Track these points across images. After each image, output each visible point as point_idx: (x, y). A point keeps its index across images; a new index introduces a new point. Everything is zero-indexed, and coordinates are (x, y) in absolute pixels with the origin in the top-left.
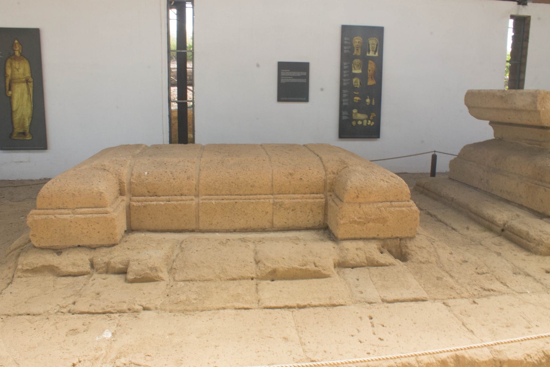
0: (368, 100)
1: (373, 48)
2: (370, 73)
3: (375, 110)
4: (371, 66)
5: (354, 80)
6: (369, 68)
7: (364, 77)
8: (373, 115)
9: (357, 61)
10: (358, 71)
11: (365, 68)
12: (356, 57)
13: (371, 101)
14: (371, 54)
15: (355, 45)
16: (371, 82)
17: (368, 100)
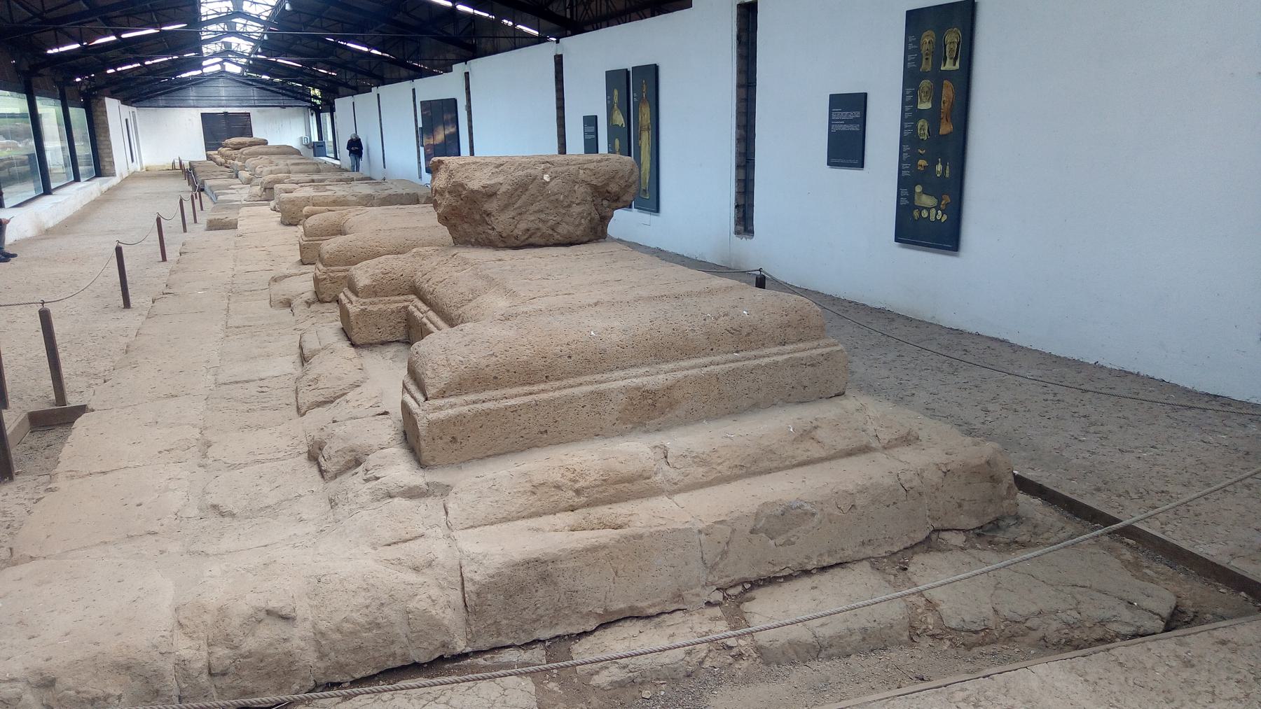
0: (939, 168)
1: (951, 50)
2: (945, 107)
3: (952, 190)
4: (948, 92)
5: (920, 123)
6: (944, 98)
7: (934, 117)
8: (946, 199)
9: (925, 84)
10: (925, 105)
11: (937, 100)
12: (925, 75)
13: (944, 169)
14: (948, 66)
15: (925, 48)
16: (946, 128)
17: (939, 168)
